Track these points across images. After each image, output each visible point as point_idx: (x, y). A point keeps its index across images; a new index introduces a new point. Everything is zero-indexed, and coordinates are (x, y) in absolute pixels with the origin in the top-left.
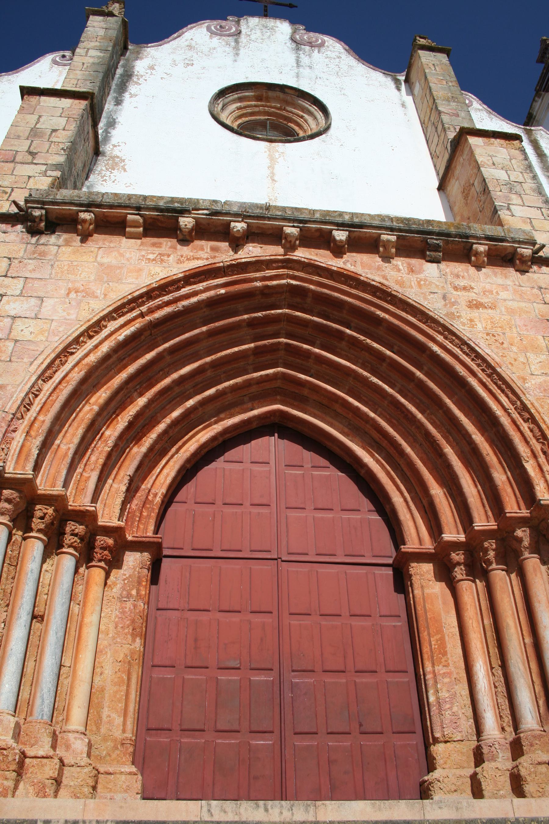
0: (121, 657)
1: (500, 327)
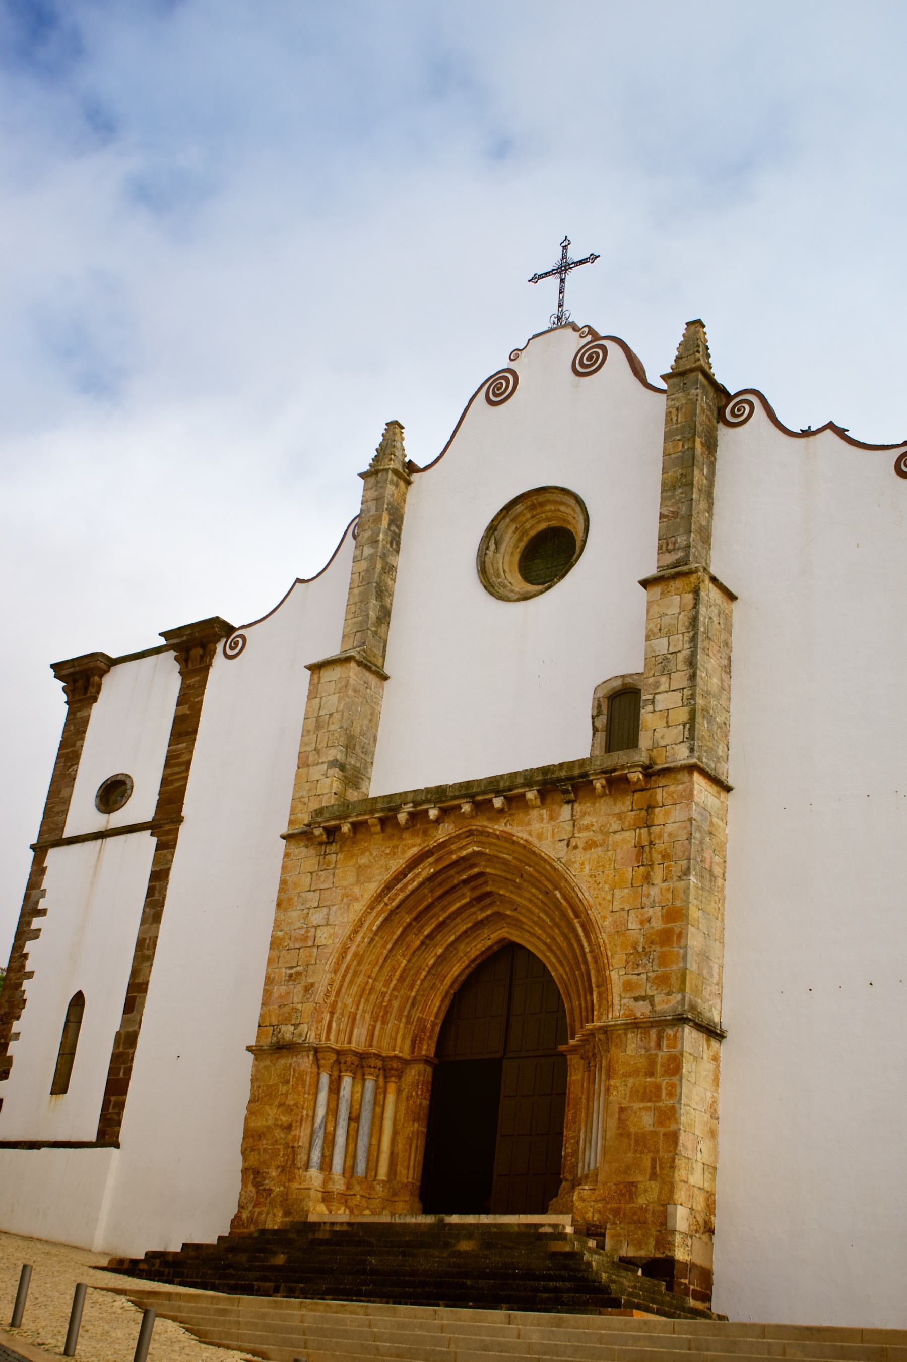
0: (406, 1136)
1: (602, 866)
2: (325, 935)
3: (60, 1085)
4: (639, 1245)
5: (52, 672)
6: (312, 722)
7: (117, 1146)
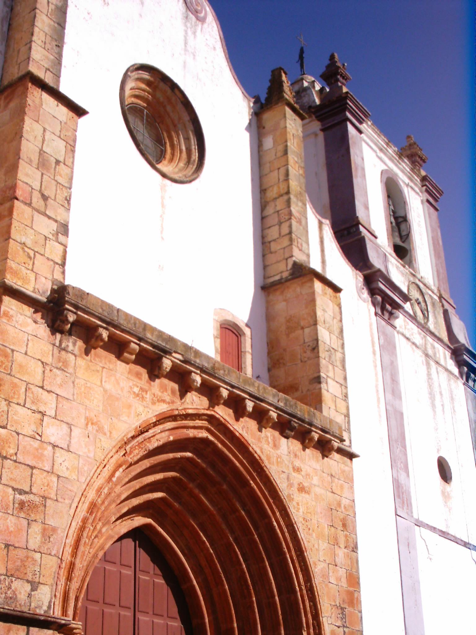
2: (66, 464)
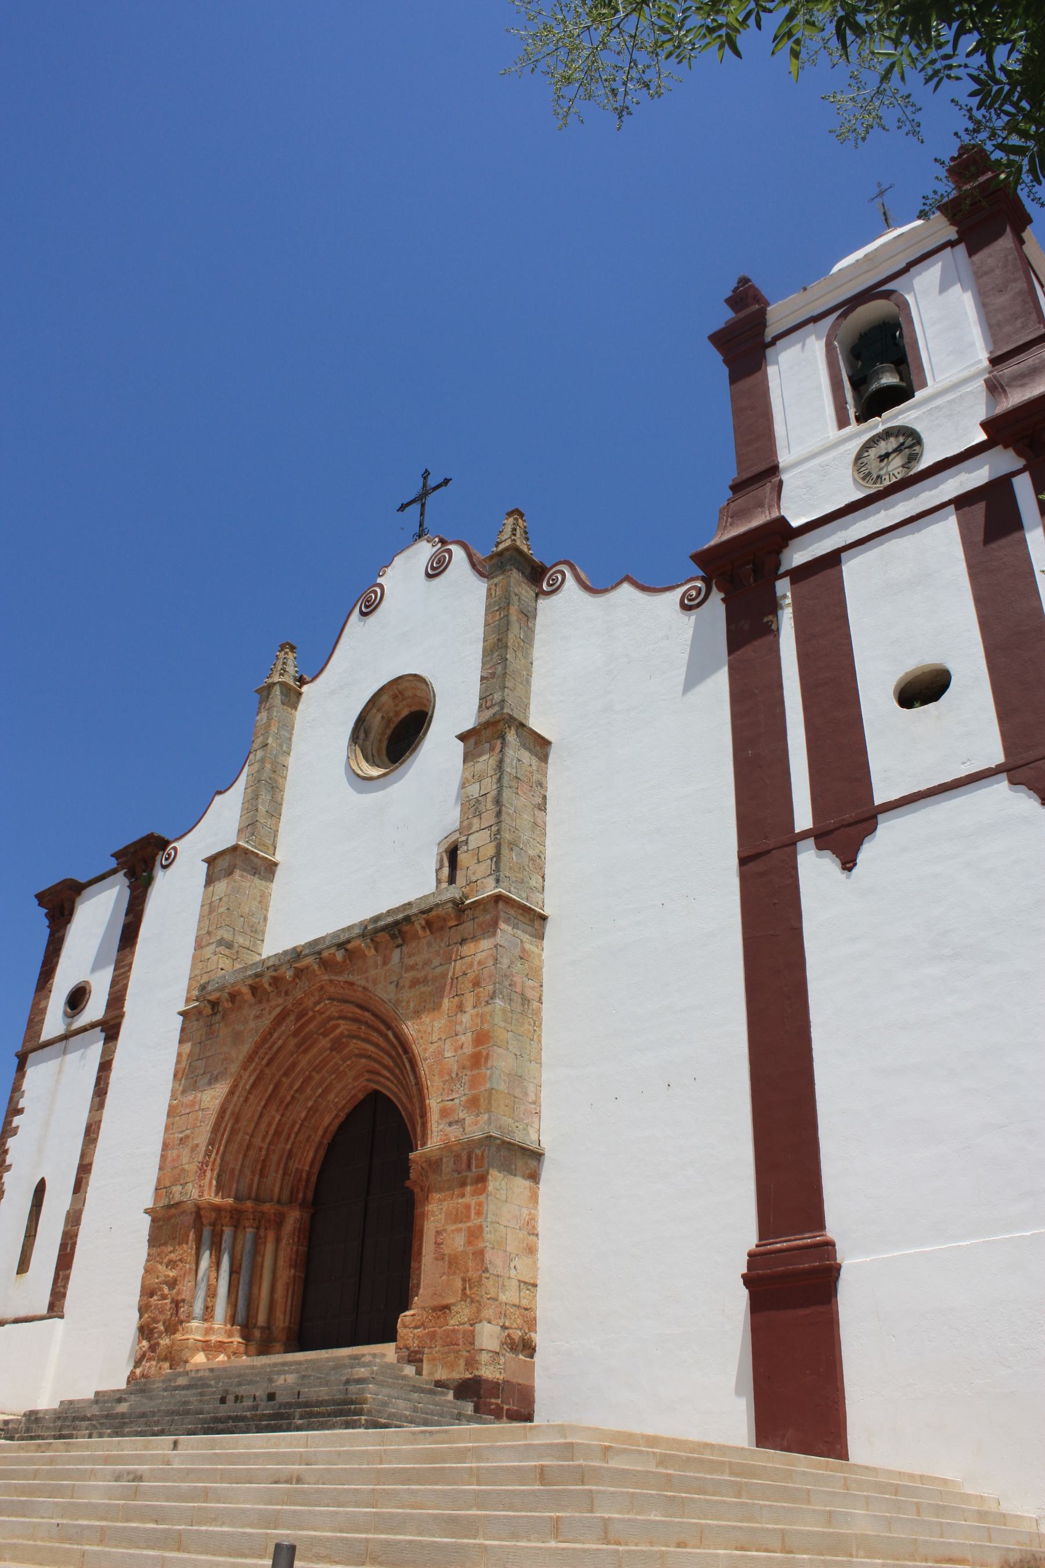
3: (23, 1266)
4: (451, 1367)
5: (36, 902)
6: (207, 907)
7: (62, 1317)
